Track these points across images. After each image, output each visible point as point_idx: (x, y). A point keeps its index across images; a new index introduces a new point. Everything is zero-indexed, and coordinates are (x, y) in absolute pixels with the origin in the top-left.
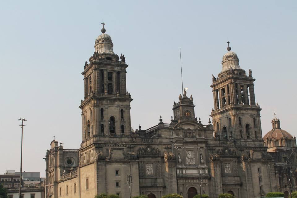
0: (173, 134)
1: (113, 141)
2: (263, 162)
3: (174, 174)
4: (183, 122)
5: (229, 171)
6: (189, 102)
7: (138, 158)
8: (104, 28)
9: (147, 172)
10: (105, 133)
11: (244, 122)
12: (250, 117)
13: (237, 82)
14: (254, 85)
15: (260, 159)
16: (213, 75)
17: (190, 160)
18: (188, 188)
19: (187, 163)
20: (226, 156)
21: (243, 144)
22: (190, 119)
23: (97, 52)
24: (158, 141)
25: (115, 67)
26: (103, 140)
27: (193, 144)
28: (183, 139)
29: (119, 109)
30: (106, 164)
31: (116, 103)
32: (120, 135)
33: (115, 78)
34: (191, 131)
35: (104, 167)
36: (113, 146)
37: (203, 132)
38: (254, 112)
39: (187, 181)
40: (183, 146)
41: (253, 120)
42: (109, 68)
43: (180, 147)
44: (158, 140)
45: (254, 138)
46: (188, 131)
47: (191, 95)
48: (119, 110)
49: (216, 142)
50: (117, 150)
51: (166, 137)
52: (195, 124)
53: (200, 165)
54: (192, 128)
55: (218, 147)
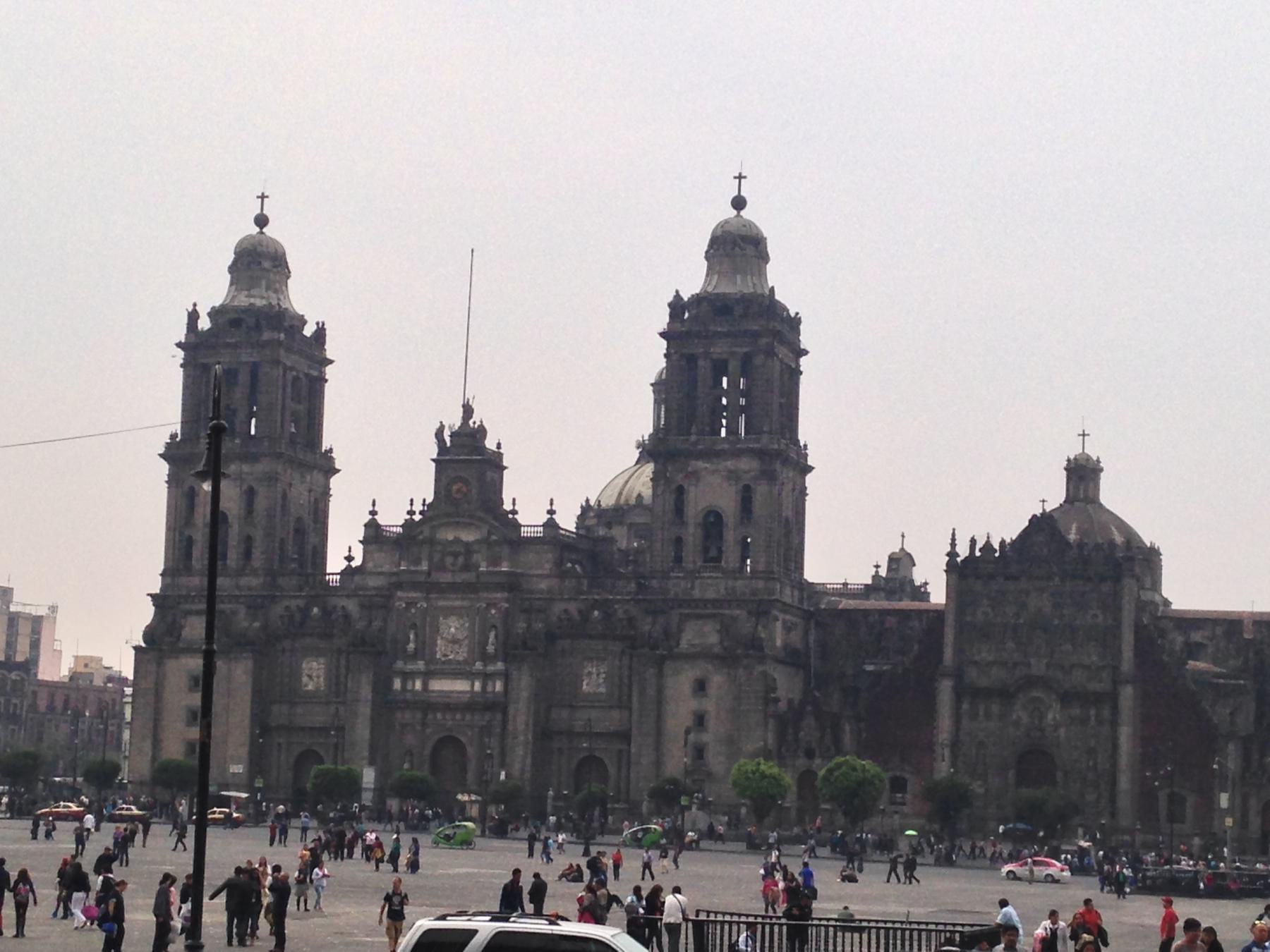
3: (366, 692)
5: (599, 685)
8: (264, 212)
9: (304, 684)
18: (436, 737)
21: (677, 586)
22: (466, 506)
32: (235, 567)
37: (506, 550)
38: (747, 465)
39: (430, 716)
40: (427, 599)
43: (411, 604)
48: (238, 489)
51: (379, 570)
53: (478, 665)
54: (468, 536)
55: (562, 600)
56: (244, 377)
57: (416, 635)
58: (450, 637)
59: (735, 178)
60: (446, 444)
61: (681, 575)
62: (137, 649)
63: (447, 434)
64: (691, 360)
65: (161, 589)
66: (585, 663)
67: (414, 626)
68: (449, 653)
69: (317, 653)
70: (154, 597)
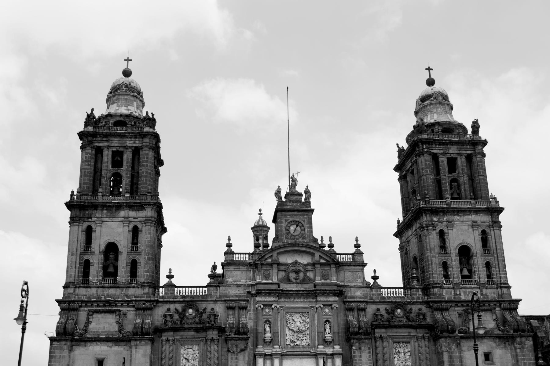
0: (254, 276)
1: (108, 294)
2: (499, 337)
4: (280, 247)
6: (300, 201)
7: (158, 331)
8: (129, 68)
10: (91, 278)
11: (453, 244)
12: (471, 230)
13: (435, 151)
14: (484, 155)
15: (492, 330)
16: (397, 145)
17: (295, 334)
19: (288, 342)
20: (396, 324)
21: (448, 294)
22: (301, 239)
23: (92, 113)
24: (218, 292)
25: (129, 140)
26: (84, 294)
27: (304, 298)
28: (279, 287)
29: (128, 226)
30: (72, 346)
31: (122, 213)
33: (127, 163)
34: (301, 268)
35: (66, 353)
36: (104, 306)
37: (333, 269)
41: (478, 238)
42: (115, 143)
44: (217, 290)
45: (484, 279)
46: (292, 268)
47: (307, 187)
48: (127, 228)
49: (372, 291)
50: (103, 315)
51: (238, 283)
52: (312, 251)
53: (321, 349)
55: (374, 302)
56: (127, 156)
57: (270, 327)
58: (295, 329)
59: (426, 69)
60: (281, 199)
61: (451, 286)
62: (52, 339)
63: (283, 194)
64: (435, 157)
65: (63, 298)
66: (395, 345)
67: (268, 321)
68: (296, 341)
69: (192, 342)
70: (58, 301)
